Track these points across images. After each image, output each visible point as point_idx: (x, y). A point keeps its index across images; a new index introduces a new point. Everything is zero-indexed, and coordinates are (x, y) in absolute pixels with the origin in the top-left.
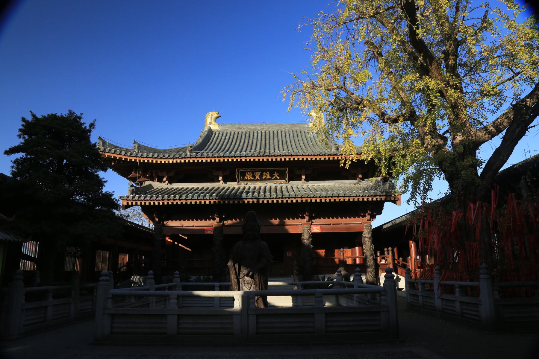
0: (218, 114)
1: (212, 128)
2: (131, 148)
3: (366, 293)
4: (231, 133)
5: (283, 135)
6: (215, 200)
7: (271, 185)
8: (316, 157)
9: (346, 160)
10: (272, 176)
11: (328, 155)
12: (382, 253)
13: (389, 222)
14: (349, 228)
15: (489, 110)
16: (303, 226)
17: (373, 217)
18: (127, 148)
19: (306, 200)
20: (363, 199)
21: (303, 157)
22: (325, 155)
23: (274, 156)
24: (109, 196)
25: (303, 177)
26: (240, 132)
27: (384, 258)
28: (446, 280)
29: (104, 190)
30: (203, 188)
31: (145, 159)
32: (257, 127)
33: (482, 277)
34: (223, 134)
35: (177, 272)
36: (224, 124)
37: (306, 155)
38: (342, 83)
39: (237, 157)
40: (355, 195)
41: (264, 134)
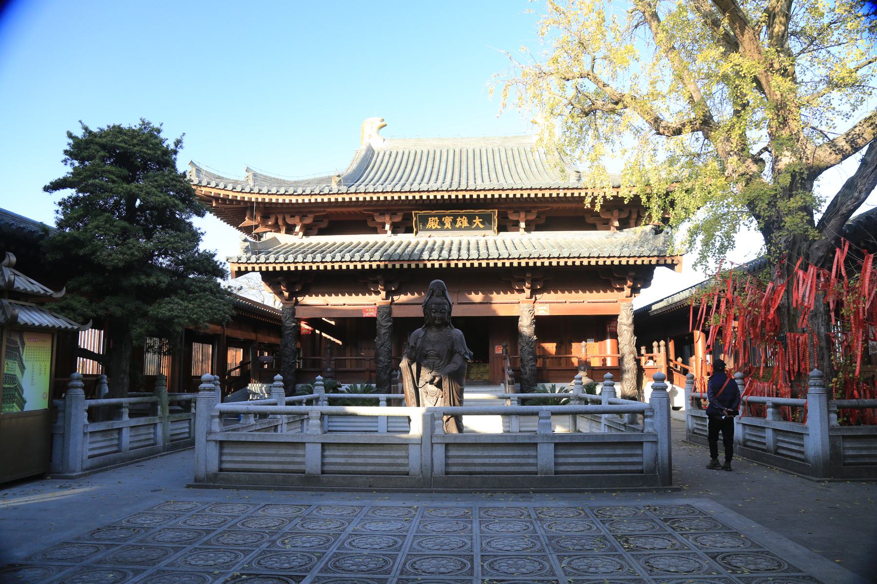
0: (383, 120)
2: (242, 178)
3: (620, 413)
6: (378, 263)
7: (470, 238)
8: (543, 192)
9: (595, 198)
11: (564, 189)
12: (650, 350)
13: (662, 300)
15: (839, 113)
17: (635, 290)
18: (237, 178)
19: (527, 263)
20: (620, 262)
21: (522, 192)
22: (558, 189)
23: (475, 190)
24: (208, 257)
25: (523, 225)
27: (651, 358)
28: (751, 395)
29: (203, 246)
30: (359, 243)
31: (264, 196)
33: (811, 390)
34: (390, 156)
35: (319, 377)
38: (589, 68)
39: (415, 192)
41: (457, 154)
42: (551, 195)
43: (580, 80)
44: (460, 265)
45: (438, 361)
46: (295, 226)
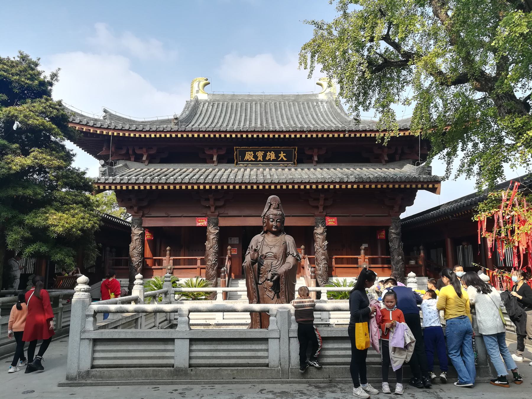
0: (207, 80)
1: (199, 99)
18: (96, 117)
25: (316, 159)
29: (75, 165)
45: (276, 261)
46: (142, 156)
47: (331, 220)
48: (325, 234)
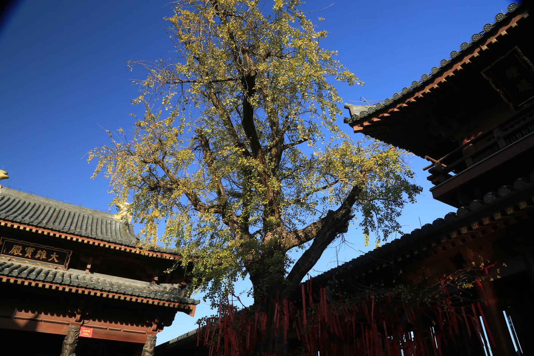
0: (7, 174)
4: (14, 200)
5: (81, 219)
8: (110, 244)
10: (48, 256)
11: (125, 246)
14: (128, 337)
16: (70, 326)
17: (160, 328)
19: (83, 292)
20: (153, 302)
22: (122, 245)
25: (89, 266)
26: (27, 203)
32: (51, 202)
36: (9, 187)
37: (99, 240)
40: (144, 296)
42: (115, 247)
43: (154, 166)
44: (26, 283)
47: (87, 331)
48: (76, 345)
